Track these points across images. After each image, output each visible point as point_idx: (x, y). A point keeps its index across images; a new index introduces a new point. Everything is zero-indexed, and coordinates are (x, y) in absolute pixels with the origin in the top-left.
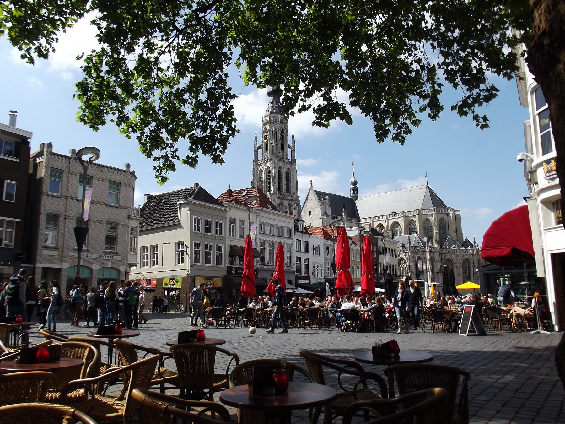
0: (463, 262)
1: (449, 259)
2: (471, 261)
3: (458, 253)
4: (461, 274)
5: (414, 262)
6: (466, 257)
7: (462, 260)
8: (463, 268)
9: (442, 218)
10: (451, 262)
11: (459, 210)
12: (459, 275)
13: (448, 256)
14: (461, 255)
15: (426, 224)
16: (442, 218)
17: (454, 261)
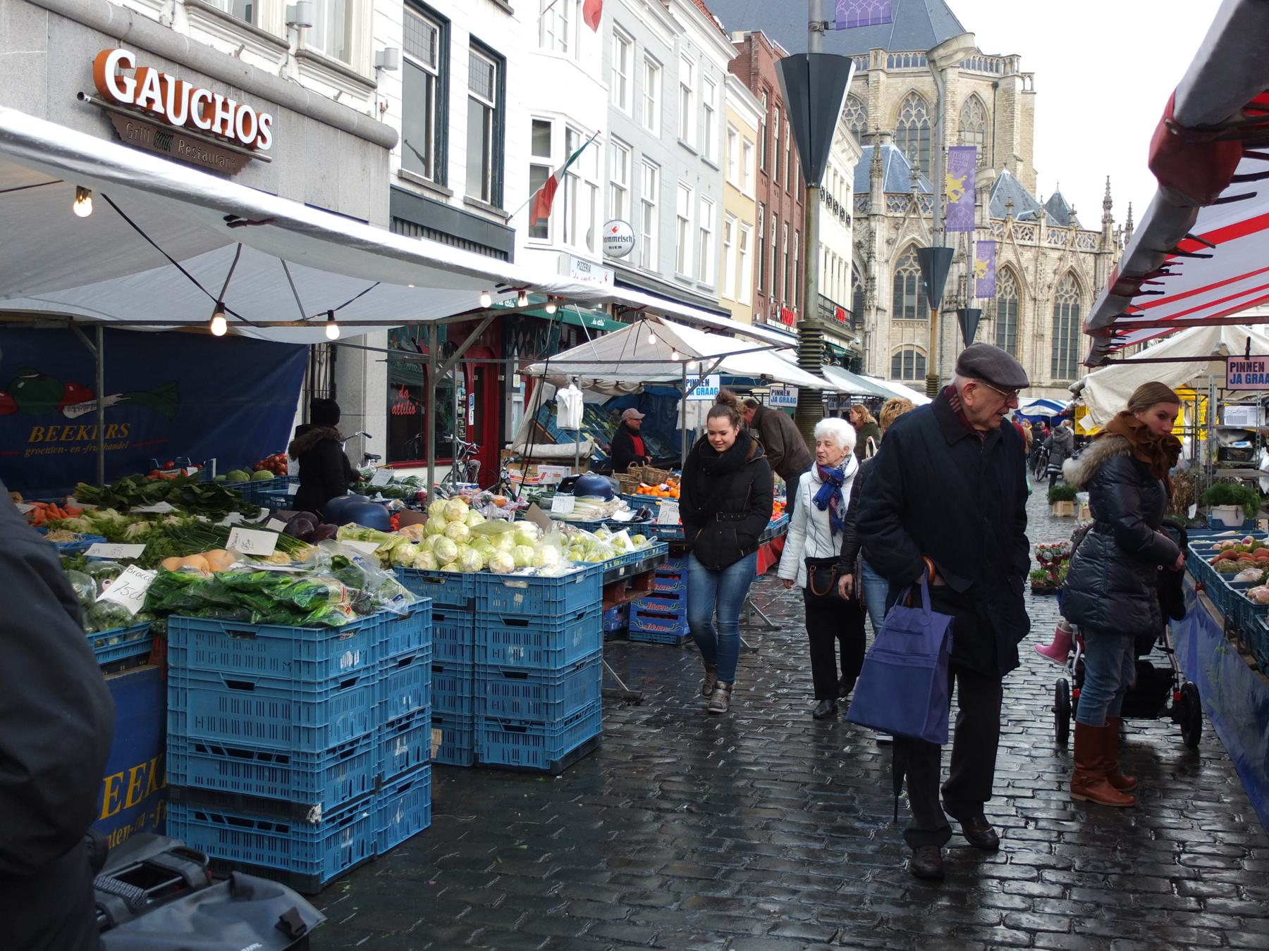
0: (1061, 284)
1: (1008, 267)
2: (1089, 282)
3: (1045, 244)
4: (1048, 333)
5: (892, 263)
6: (1071, 262)
7: (1055, 273)
8: (1057, 308)
9: (974, 96)
10: (1016, 280)
11: (1030, 75)
12: (1039, 336)
13: (1007, 255)
14: (1056, 254)
15: (908, 115)
16: (974, 96)
17: (1030, 278)
